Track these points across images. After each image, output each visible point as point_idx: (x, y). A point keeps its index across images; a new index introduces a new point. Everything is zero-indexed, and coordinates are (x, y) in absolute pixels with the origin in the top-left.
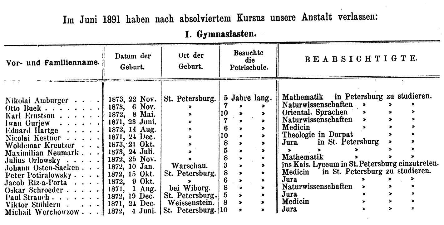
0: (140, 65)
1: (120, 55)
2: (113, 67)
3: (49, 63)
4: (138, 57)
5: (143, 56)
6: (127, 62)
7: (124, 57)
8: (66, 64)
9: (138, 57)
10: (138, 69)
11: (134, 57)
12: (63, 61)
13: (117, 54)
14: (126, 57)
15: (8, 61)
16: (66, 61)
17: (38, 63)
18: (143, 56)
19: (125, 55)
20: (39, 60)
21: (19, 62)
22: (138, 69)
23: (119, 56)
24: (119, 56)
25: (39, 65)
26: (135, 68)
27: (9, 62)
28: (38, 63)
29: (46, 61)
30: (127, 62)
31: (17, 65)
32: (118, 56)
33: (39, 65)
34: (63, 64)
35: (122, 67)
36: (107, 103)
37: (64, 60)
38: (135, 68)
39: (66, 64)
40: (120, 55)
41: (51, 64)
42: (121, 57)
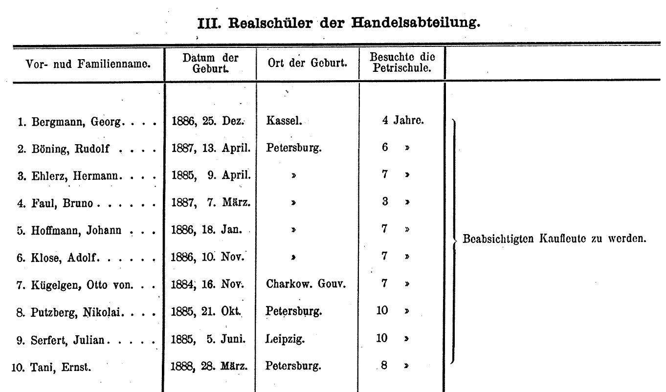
3: (85, 64)
7: (197, 58)
8: (107, 66)
11: (212, 58)
12: (103, 62)
13: (185, 54)
15: (28, 61)
16: (107, 61)
17: (68, 65)
18: (226, 58)
19: (198, 56)
25: (70, 67)
27: (30, 62)
28: (69, 64)
31: (41, 67)
33: (70, 67)
34: (103, 66)
37: (105, 60)
39: (107, 66)
42: (192, 59)
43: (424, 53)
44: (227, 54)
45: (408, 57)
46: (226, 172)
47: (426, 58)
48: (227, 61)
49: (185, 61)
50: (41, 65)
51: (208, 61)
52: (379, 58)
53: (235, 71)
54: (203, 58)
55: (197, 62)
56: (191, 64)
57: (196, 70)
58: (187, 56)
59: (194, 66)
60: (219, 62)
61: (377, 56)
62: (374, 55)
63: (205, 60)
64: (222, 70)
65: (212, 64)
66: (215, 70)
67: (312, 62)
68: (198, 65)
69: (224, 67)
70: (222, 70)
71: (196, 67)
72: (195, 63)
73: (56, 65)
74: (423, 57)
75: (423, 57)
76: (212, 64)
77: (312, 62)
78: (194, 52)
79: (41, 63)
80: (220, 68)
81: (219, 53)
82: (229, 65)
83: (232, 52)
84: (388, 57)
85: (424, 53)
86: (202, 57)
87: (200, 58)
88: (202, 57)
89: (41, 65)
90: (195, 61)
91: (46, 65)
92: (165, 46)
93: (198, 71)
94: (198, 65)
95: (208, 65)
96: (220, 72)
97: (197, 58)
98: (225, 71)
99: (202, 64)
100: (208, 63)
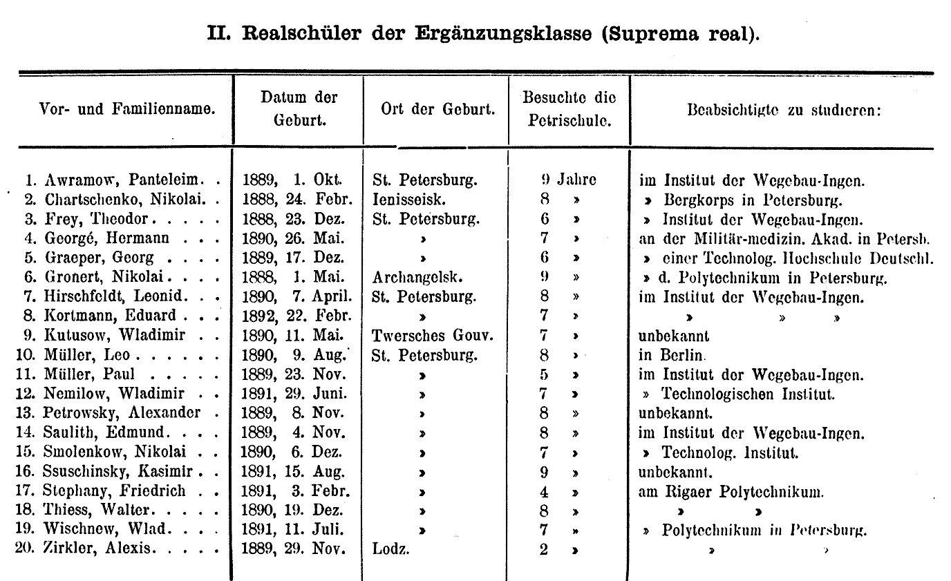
0: (317, 117)
1: (271, 94)
2: (256, 121)
4: (311, 98)
5: (322, 98)
6: (288, 110)
7: (281, 98)
9: (311, 98)
10: (313, 125)
14: (286, 97)
18: (322, 98)
19: (283, 95)
22: (313, 125)
23: (267, 97)
24: (267, 97)
26: (305, 122)
30: (288, 110)
35: (279, 121)
36: (240, 190)
38: (305, 122)
40: (271, 94)
42: (273, 98)
43: (600, 92)
45: (578, 98)
46: (319, 467)
47: (603, 100)
49: (264, 101)
52: (536, 98)
61: (533, 96)
62: (529, 94)
67: (445, 106)
74: (599, 98)
75: (598, 97)
77: (445, 106)
84: (548, 98)
85: (600, 92)
87: (286, 97)
97: (281, 98)
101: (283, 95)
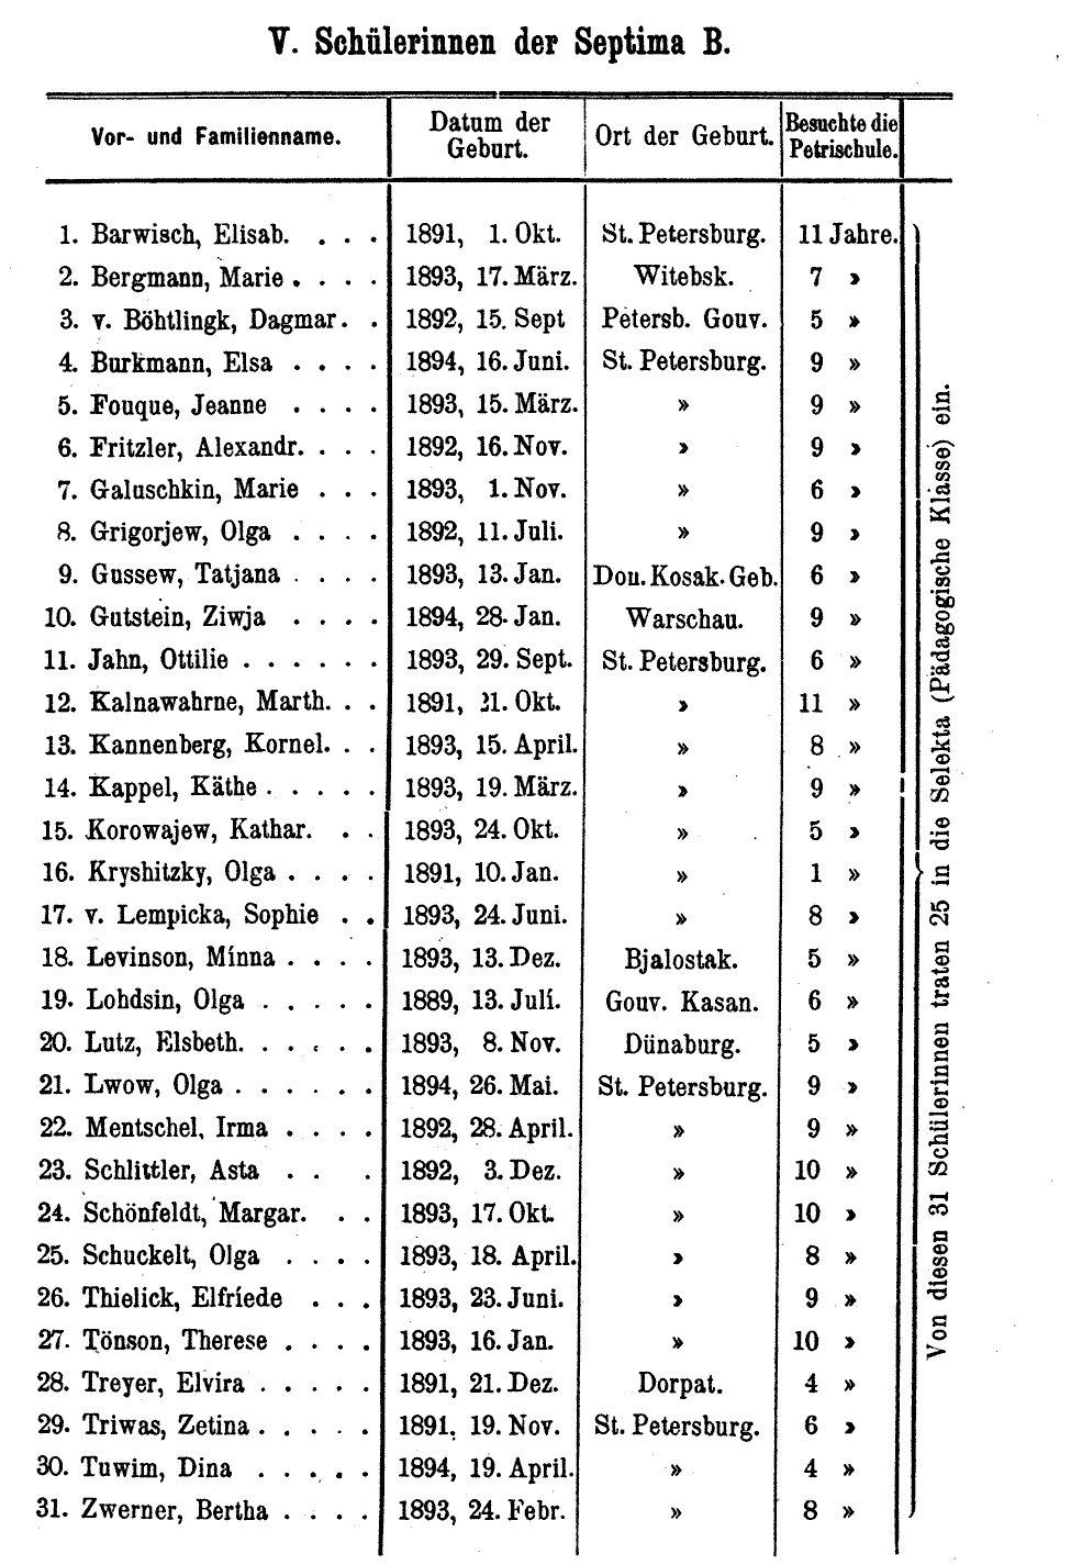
5: (524, 123)
7: (461, 124)
11: (494, 124)
14: (469, 122)
18: (524, 123)
19: (465, 118)
20: (179, 129)
21: (124, 135)
24: (439, 122)
28: (176, 137)
29: (199, 129)
32: (440, 124)
41: (213, 140)
42: (449, 124)
44: (524, 113)
48: (525, 129)
50: (115, 139)
51: (487, 130)
53: (543, 153)
54: (476, 124)
55: (461, 134)
56: (447, 134)
57: (456, 152)
58: (439, 118)
59: (451, 142)
60: (509, 134)
63: (480, 129)
64: (512, 151)
65: (490, 138)
66: (498, 152)
68: (461, 141)
69: (518, 144)
70: (512, 151)
71: (456, 143)
72: (456, 134)
73: (153, 139)
76: (490, 138)
78: (454, 108)
79: (121, 135)
80: (508, 146)
81: (509, 111)
82: (528, 140)
83: (536, 108)
86: (473, 119)
87: (469, 122)
88: (473, 119)
89: (115, 139)
90: (458, 129)
91: (130, 139)
92: (389, 96)
93: (460, 155)
94: (461, 141)
95: (480, 139)
96: (507, 156)
98: (519, 155)
99: (470, 138)
100: (484, 134)
101: (465, 118)
